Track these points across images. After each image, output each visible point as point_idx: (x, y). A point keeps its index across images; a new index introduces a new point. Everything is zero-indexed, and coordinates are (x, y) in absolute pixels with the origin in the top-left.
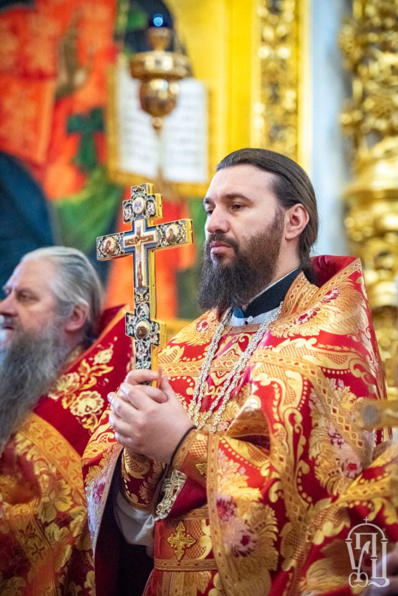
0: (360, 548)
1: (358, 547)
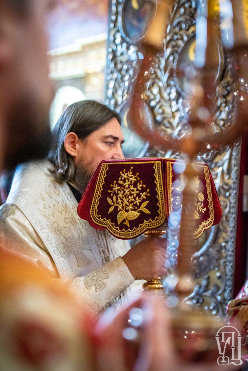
0: (224, 341)
1: (223, 340)
